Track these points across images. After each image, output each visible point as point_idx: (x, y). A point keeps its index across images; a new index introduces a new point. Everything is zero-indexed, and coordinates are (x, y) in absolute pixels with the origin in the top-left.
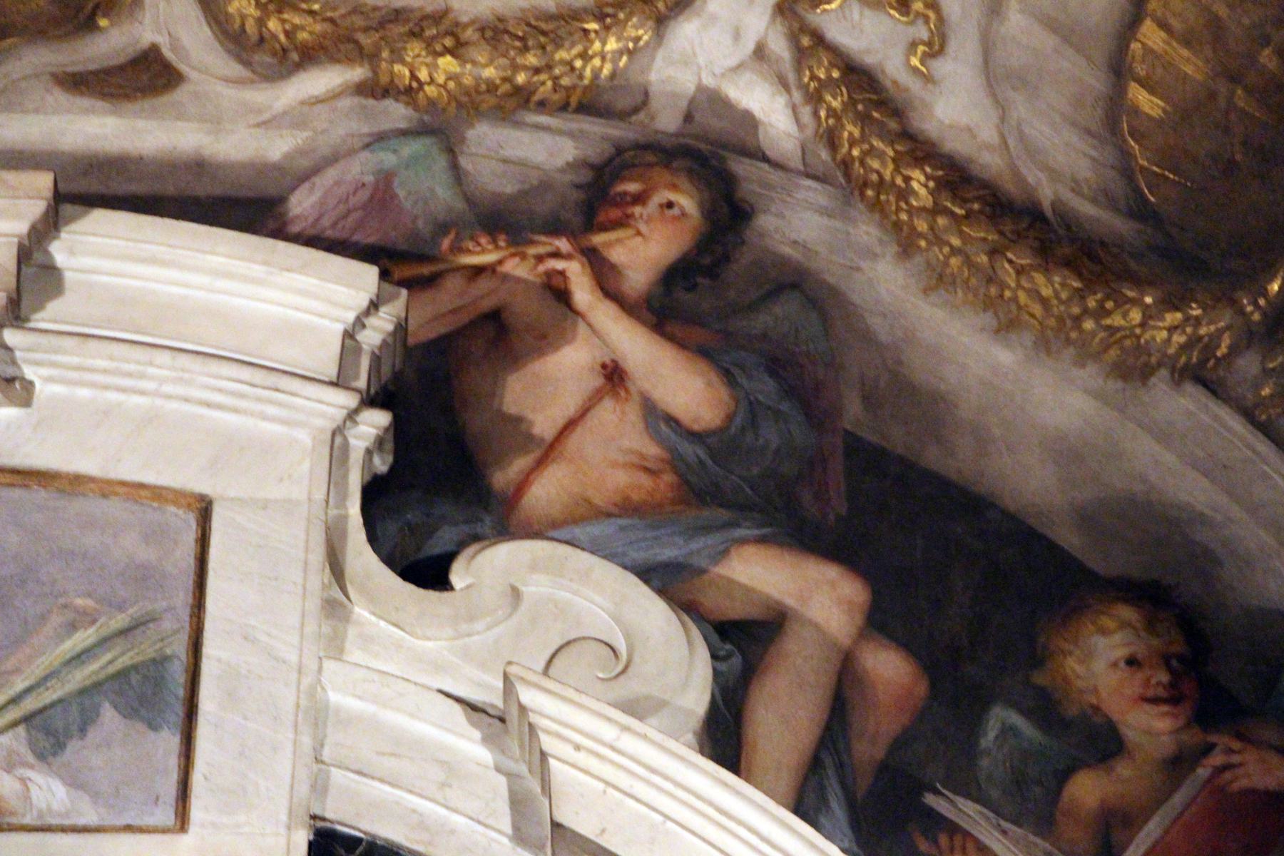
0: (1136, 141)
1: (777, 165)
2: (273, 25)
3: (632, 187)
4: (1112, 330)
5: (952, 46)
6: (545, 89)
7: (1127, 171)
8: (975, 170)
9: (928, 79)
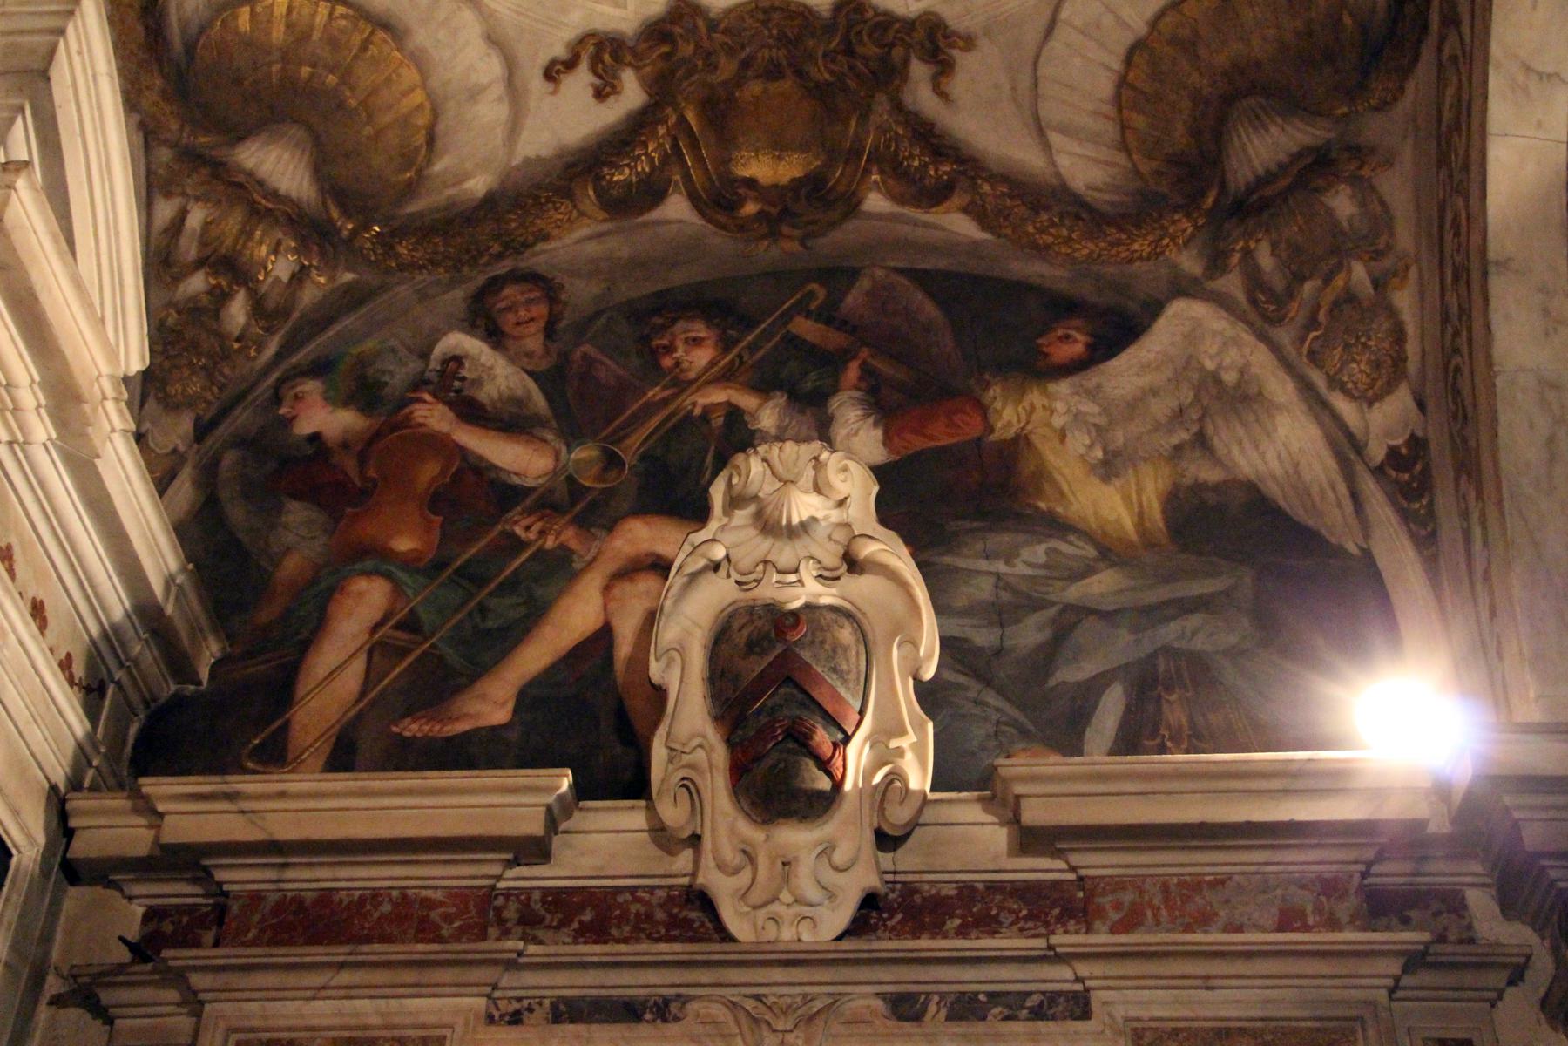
7: (202, 30)
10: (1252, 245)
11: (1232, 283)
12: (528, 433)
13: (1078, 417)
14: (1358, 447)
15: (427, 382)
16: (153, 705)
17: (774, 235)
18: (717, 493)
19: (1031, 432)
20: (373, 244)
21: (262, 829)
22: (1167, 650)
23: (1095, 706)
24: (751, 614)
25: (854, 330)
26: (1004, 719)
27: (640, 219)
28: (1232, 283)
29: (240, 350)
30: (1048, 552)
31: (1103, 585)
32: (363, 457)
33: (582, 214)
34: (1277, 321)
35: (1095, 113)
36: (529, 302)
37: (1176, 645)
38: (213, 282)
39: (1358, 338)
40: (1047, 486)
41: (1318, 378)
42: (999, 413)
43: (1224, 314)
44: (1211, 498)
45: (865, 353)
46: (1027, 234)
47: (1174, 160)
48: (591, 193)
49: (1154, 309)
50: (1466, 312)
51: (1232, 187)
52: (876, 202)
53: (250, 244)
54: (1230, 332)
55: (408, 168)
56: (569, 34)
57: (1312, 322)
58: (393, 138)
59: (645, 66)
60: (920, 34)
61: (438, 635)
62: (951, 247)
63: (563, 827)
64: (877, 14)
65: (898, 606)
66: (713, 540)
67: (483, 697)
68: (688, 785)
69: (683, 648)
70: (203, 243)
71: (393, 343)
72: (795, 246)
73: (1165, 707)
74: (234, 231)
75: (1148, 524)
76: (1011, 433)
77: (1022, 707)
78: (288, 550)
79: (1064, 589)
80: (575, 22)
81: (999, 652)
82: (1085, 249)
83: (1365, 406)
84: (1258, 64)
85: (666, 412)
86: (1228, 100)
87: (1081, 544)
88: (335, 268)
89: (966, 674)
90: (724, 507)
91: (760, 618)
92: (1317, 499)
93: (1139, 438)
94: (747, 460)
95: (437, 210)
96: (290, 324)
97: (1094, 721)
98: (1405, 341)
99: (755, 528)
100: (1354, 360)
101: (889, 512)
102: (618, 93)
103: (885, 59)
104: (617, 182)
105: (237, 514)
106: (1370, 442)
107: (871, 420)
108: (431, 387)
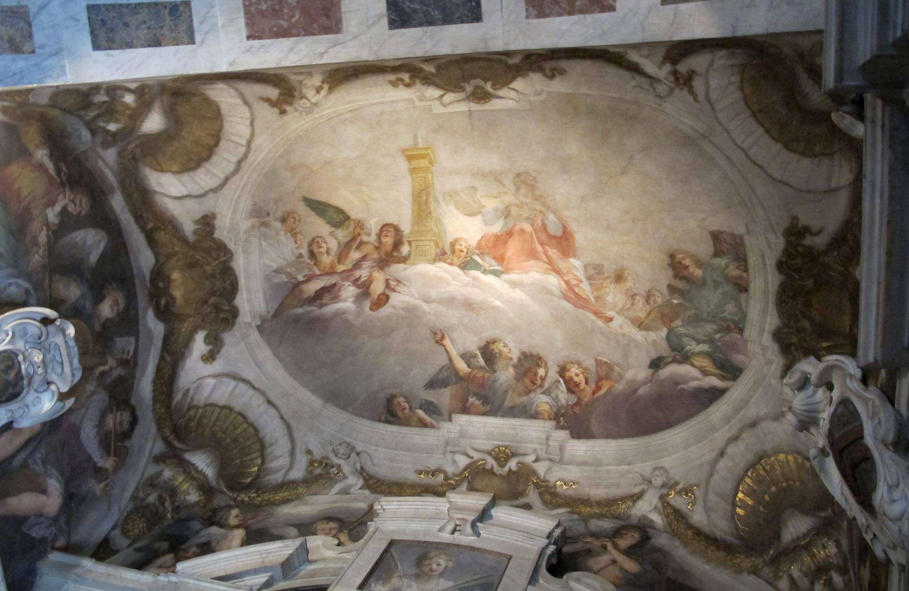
0: (739, 521)
1: (656, 529)
2: (554, 501)
3: (624, 532)
4: (733, 563)
6: (609, 515)
7: (737, 528)
38: (822, 582)
53: (817, 557)
60: (792, 239)
64: (784, 256)
70: (806, 575)
74: (809, 560)
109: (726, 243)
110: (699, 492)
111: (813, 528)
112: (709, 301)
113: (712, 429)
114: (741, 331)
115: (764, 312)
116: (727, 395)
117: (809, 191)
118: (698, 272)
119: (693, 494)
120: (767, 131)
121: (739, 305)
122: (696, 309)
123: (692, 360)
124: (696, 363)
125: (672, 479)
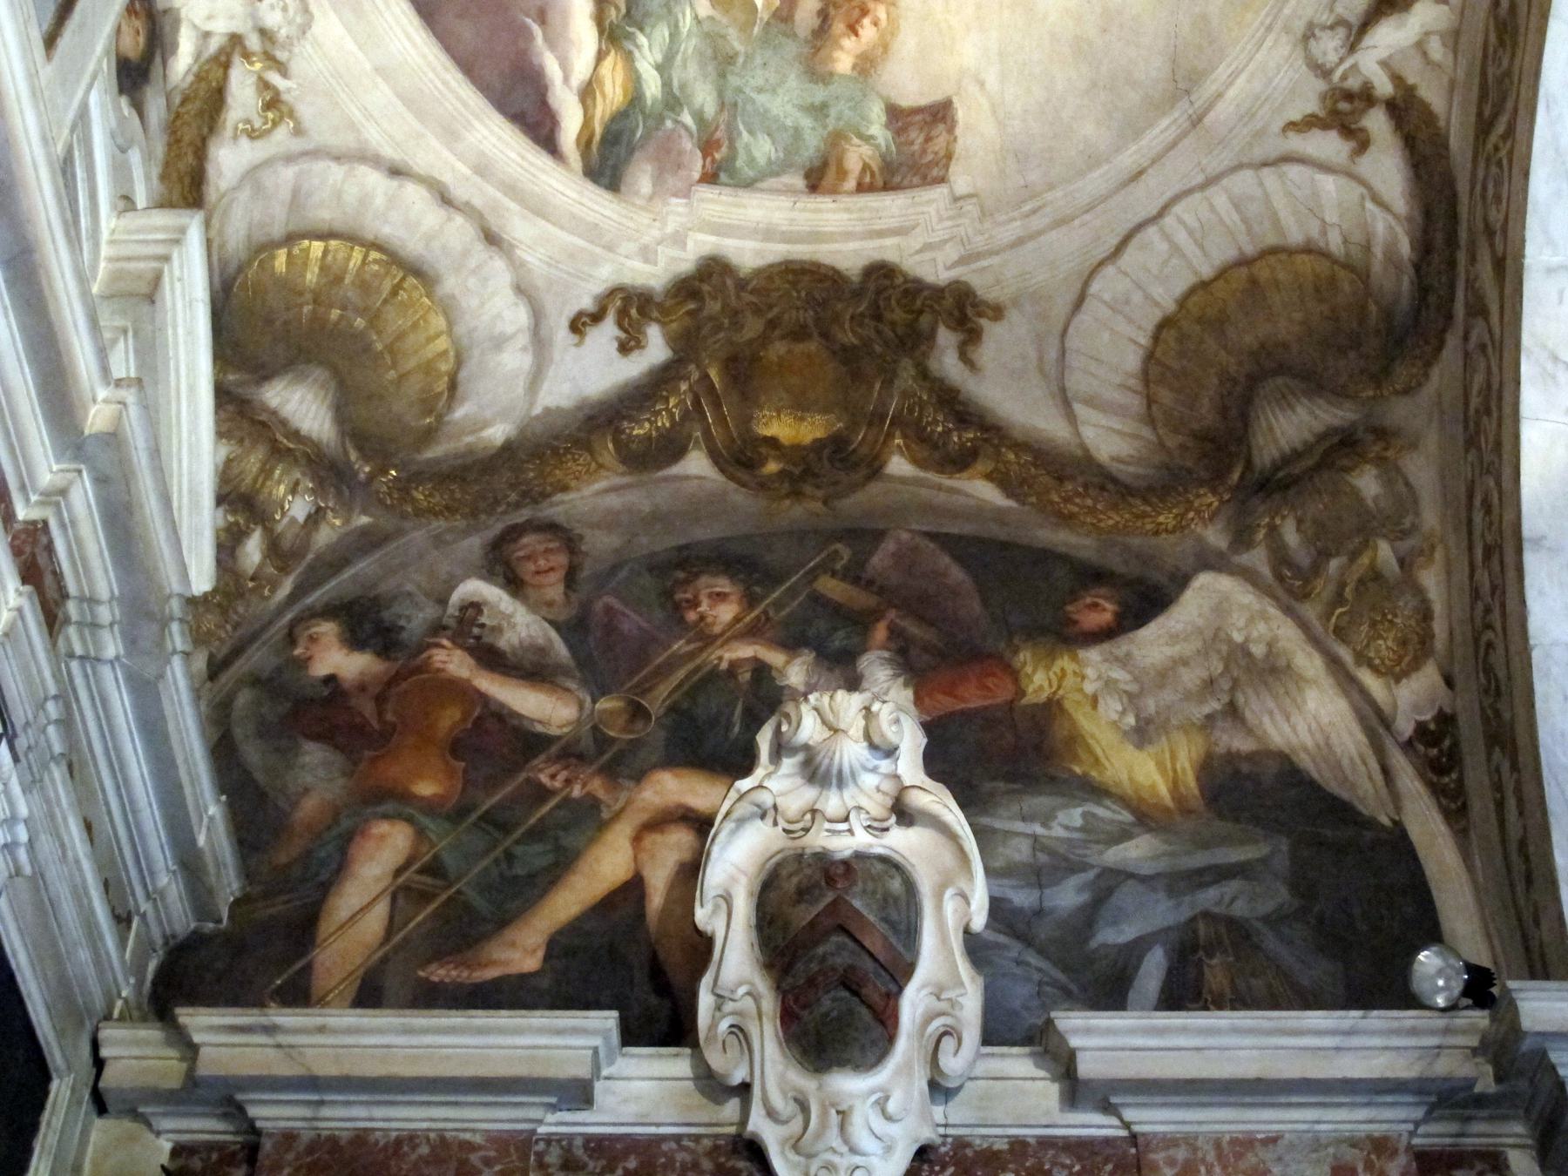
1: (165, 76)
5: (259, 144)
7: (240, 269)
8: (204, 187)
9: (235, 138)
10: (1278, 521)
11: (1257, 558)
12: (552, 682)
13: (1109, 684)
14: (1387, 722)
15: (445, 628)
16: (172, 943)
17: (796, 494)
18: (764, 739)
19: (1063, 698)
20: (389, 488)
21: (303, 1065)
22: (1206, 915)
23: (1137, 968)
24: (800, 863)
25: (881, 591)
26: (1045, 979)
27: (660, 474)
28: (1257, 558)
29: (253, 590)
30: (1084, 815)
31: (1138, 851)
32: (380, 700)
33: (601, 466)
34: (1305, 596)
35: (1123, 387)
36: (547, 551)
37: (1216, 910)
38: (231, 519)
39: (1384, 615)
40: (1083, 755)
41: (1345, 654)
42: (1030, 677)
43: (1250, 588)
44: (1245, 768)
45: (892, 614)
46: (1052, 503)
47: (1203, 437)
48: (610, 446)
49: (1182, 581)
50: (1498, 589)
51: (1257, 461)
52: (898, 466)
53: (269, 483)
54: (1256, 606)
55: (430, 412)
56: (598, 288)
57: (1339, 599)
58: (414, 386)
59: (672, 321)
60: (949, 302)
61: (465, 880)
62: (980, 511)
63: (605, 1072)
64: (906, 281)
65: (948, 858)
66: (760, 787)
67: (513, 945)
68: (738, 1030)
69: (730, 896)
71: (409, 587)
72: (817, 506)
73: (1206, 970)
74: (254, 470)
75: (1182, 789)
76: (1043, 697)
77: (1066, 969)
78: (307, 791)
79: (1101, 853)
80: (604, 275)
81: (1039, 913)
82: (1112, 519)
83: (1392, 682)
84: (1285, 346)
85: (690, 666)
86: (1254, 381)
87: (1114, 807)
88: (350, 510)
89: (1005, 934)
90: (771, 755)
91: (810, 865)
92: (1348, 772)
93: (1169, 707)
94: (798, 708)
95: (456, 456)
96: (304, 563)
97: (1136, 983)
98: (1432, 618)
99: (803, 777)
100: (1381, 637)
101: (937, 763)
102: (643, 347)
103: (912, 326)
104: (637, 436)
105: (253, 753)
106: (1399, 717)
107: (901, 680)
108: (449, 633)
109: (928, 139)
110: (282, 134)
111: (316, 445)
112: (774, 91)
113: (450, 134)
114: (710, 178)
115: (768, 234)
116: (539, 159)
117: (1063, 352)
118: (843, 61)
119: (275, 124)
120: (1203, 286)
121: (775, 169)
122: (749, 58)
123: (613, 53)
124: (608, 62)
125: (290, 51)
